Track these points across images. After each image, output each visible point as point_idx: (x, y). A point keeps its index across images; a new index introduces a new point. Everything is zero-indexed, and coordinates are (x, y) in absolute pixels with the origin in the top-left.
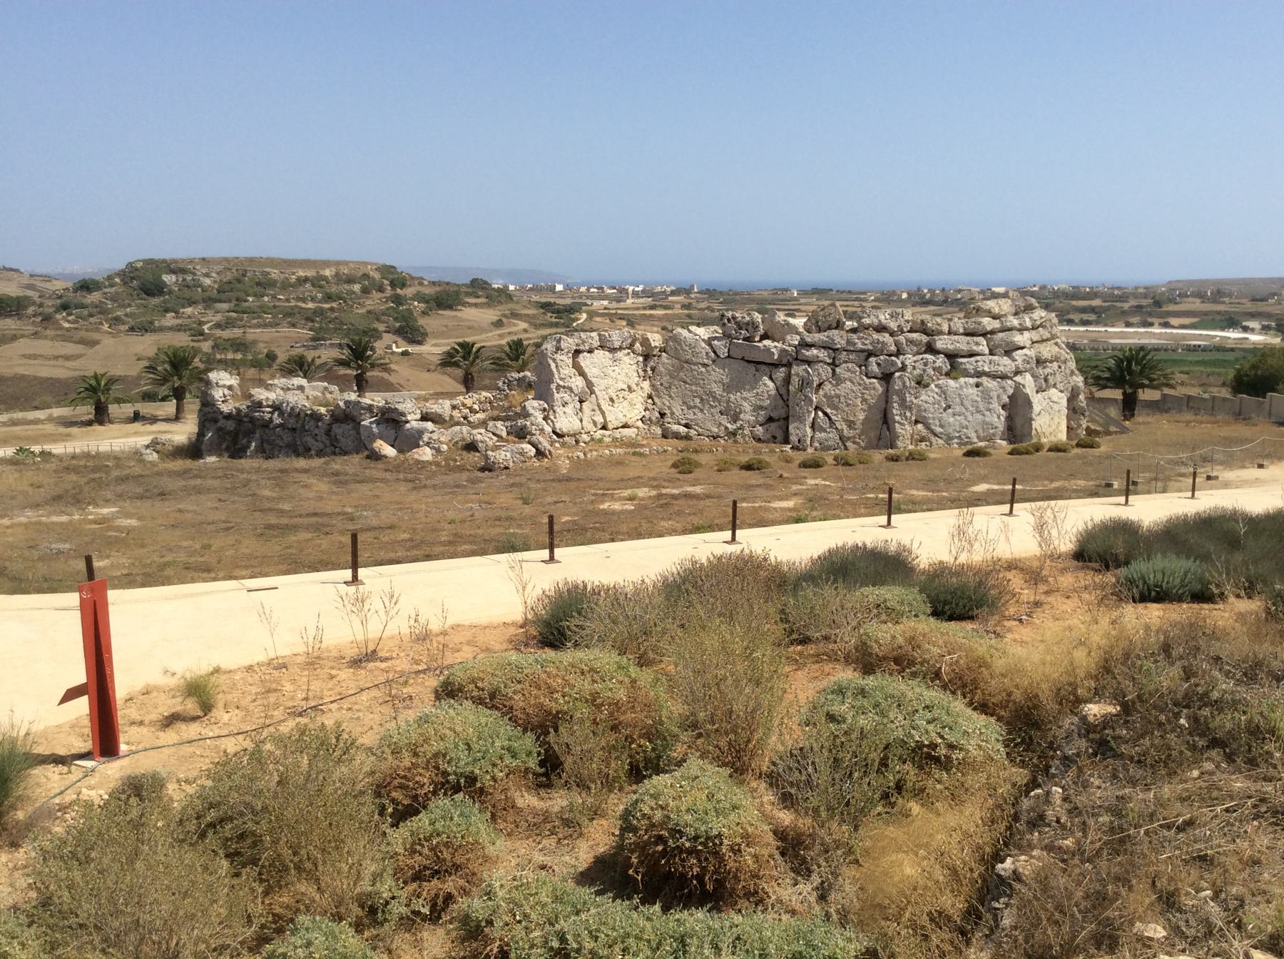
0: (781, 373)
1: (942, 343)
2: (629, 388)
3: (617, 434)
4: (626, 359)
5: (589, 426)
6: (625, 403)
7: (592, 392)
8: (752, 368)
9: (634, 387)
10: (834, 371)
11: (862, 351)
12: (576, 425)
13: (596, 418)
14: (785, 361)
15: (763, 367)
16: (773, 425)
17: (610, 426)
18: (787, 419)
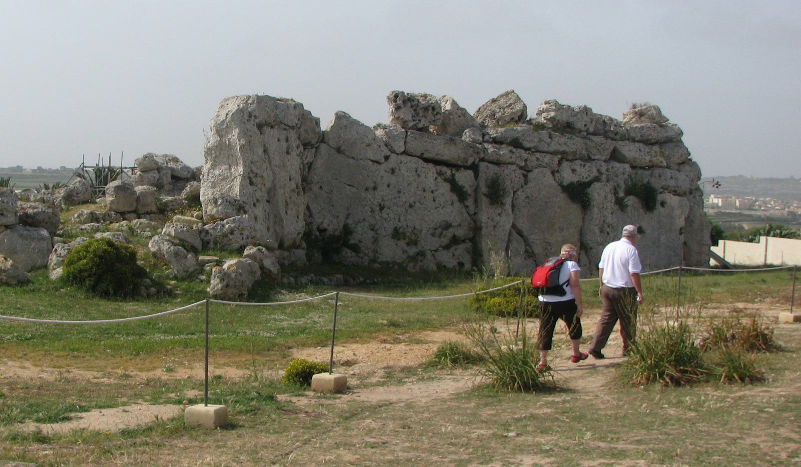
1: (629, 150)
10: (525, 176)
11: (555, 153)
16: (461, 249)
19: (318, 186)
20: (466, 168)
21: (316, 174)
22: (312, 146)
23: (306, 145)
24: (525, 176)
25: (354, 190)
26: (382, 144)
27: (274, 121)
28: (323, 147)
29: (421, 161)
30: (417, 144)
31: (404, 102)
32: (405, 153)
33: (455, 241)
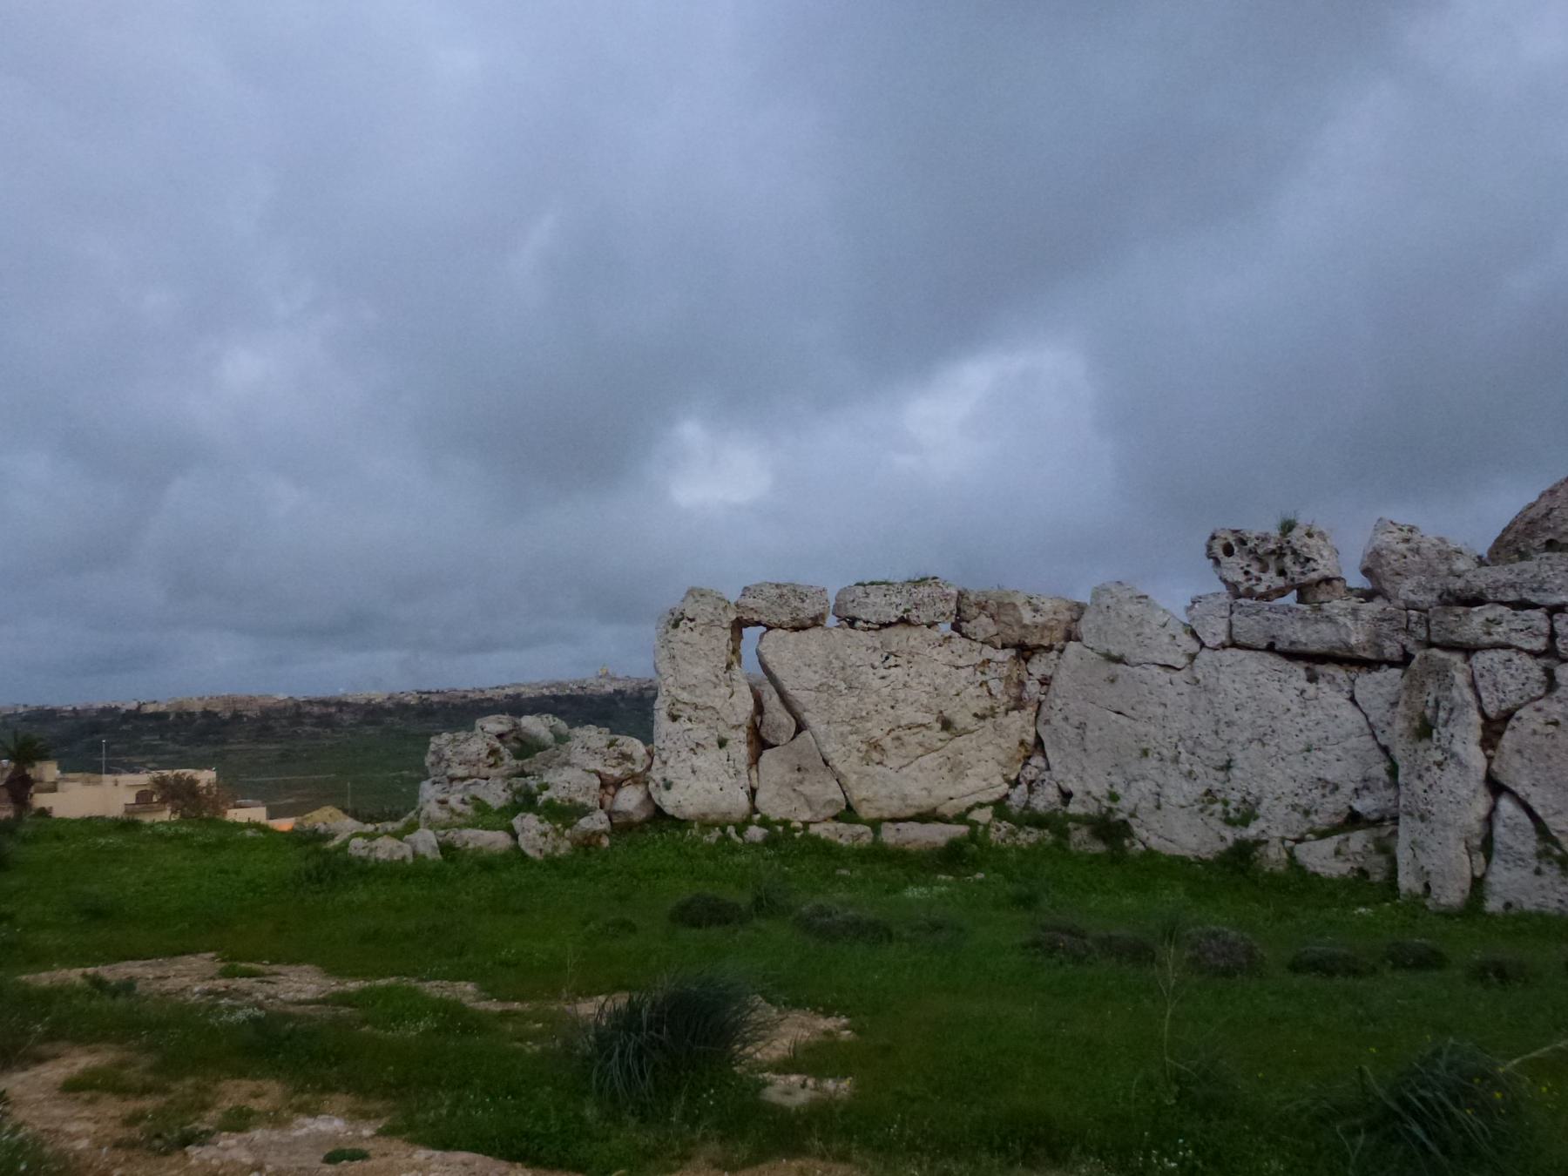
0: (1378, 686)
2: (946, 725)
3: (889, 835)
4: (942, 655)
5: (774, 804)
6: (929, 761)
7: (800, 727)
8: (1299, 669)
9: (963, 719)
10: (1549, 673)
12: (738, 801)
13: (806, 789)
14: (1391, 650)
15: (1330, 670)
16: (1358, 840)
17: (866, 811)
18: (1387, 820)
19: (1060, 716)
20: (1392, 664)
21: (1056, 695)
22: (1050, 648)
23: (1025, 652)
24: (1549, 673)
25: (1123, 720)
26: (1180, 631)
27: (794, 620)
28: (1072, 647)
29: (1270, 659)
30: (1250, 626)
31: (1228, 551)
32: (1234, 645)
33: (1354, 820)
